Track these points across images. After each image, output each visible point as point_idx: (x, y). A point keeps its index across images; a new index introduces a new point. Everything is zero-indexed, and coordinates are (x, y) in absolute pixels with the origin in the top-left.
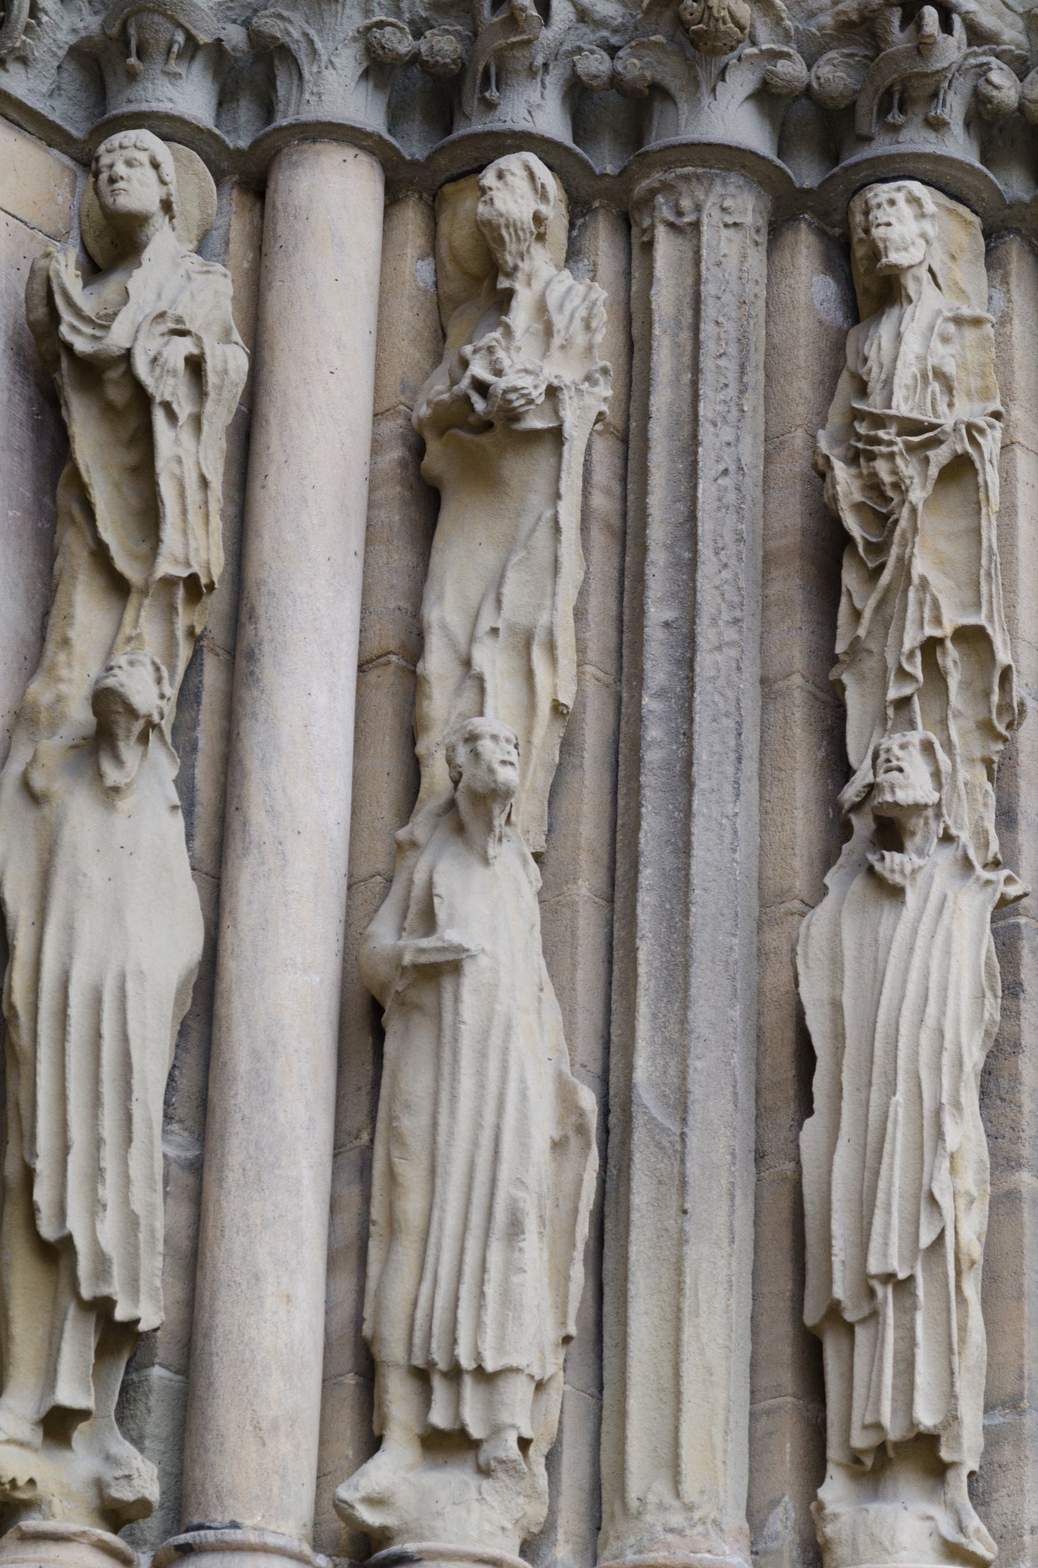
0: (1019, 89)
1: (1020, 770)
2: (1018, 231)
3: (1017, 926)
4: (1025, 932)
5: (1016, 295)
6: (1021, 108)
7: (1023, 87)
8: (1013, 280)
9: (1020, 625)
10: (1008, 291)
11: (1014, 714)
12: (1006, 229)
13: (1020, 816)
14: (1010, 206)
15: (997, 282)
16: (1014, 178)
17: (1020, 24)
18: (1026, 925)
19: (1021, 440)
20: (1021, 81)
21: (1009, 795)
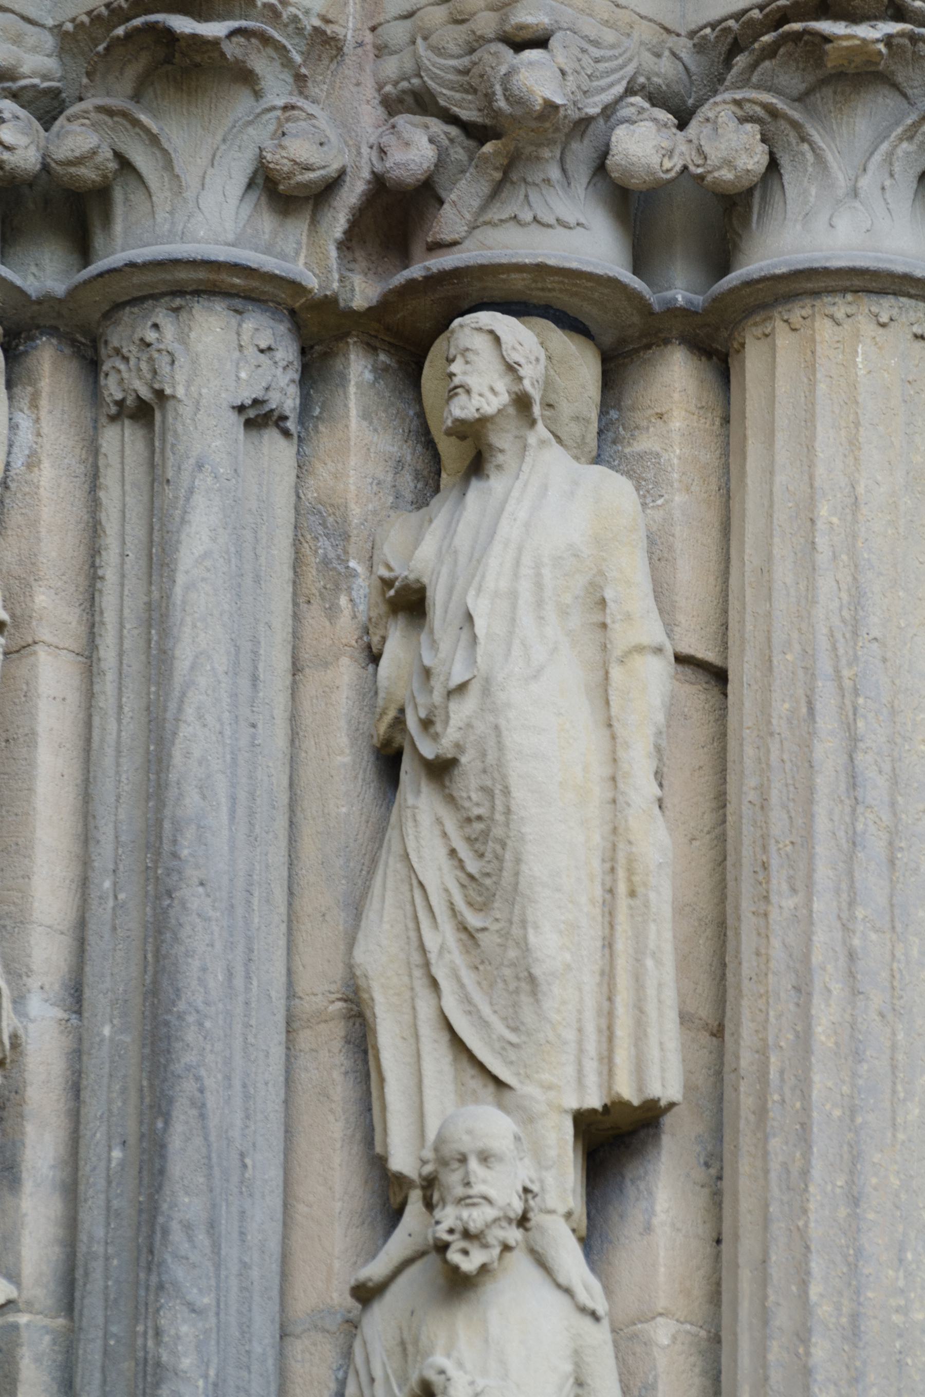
0: (43, 143)
1: (29, 1109)
2: (53, 331)
3: (15, 1327)
4: (25, 1335)
5: (46, 428)
6: (45, 167)
7: (47, 139)
8: (44, 402)
9: (36, 904)
10: (37, 420)
11: (4, 1051)
12: (38, 327)
13: (25, 1175)
14: (39, 302)
15: (25, 404)
16: (47, 256)
17: (49, 41)
18: (28, 1325)
19: (45, 638)
20: (46, 130)
21: (14, 1143)
